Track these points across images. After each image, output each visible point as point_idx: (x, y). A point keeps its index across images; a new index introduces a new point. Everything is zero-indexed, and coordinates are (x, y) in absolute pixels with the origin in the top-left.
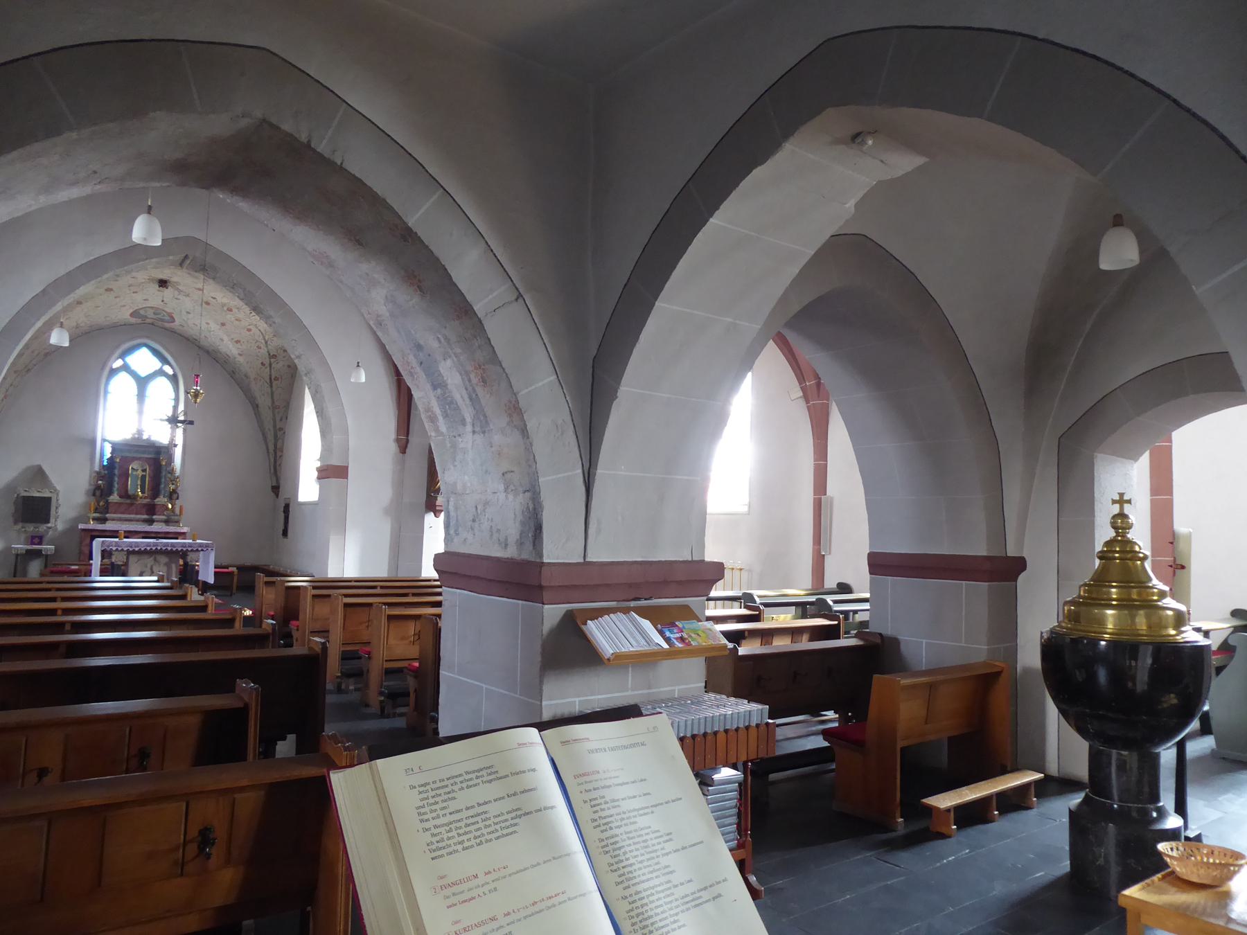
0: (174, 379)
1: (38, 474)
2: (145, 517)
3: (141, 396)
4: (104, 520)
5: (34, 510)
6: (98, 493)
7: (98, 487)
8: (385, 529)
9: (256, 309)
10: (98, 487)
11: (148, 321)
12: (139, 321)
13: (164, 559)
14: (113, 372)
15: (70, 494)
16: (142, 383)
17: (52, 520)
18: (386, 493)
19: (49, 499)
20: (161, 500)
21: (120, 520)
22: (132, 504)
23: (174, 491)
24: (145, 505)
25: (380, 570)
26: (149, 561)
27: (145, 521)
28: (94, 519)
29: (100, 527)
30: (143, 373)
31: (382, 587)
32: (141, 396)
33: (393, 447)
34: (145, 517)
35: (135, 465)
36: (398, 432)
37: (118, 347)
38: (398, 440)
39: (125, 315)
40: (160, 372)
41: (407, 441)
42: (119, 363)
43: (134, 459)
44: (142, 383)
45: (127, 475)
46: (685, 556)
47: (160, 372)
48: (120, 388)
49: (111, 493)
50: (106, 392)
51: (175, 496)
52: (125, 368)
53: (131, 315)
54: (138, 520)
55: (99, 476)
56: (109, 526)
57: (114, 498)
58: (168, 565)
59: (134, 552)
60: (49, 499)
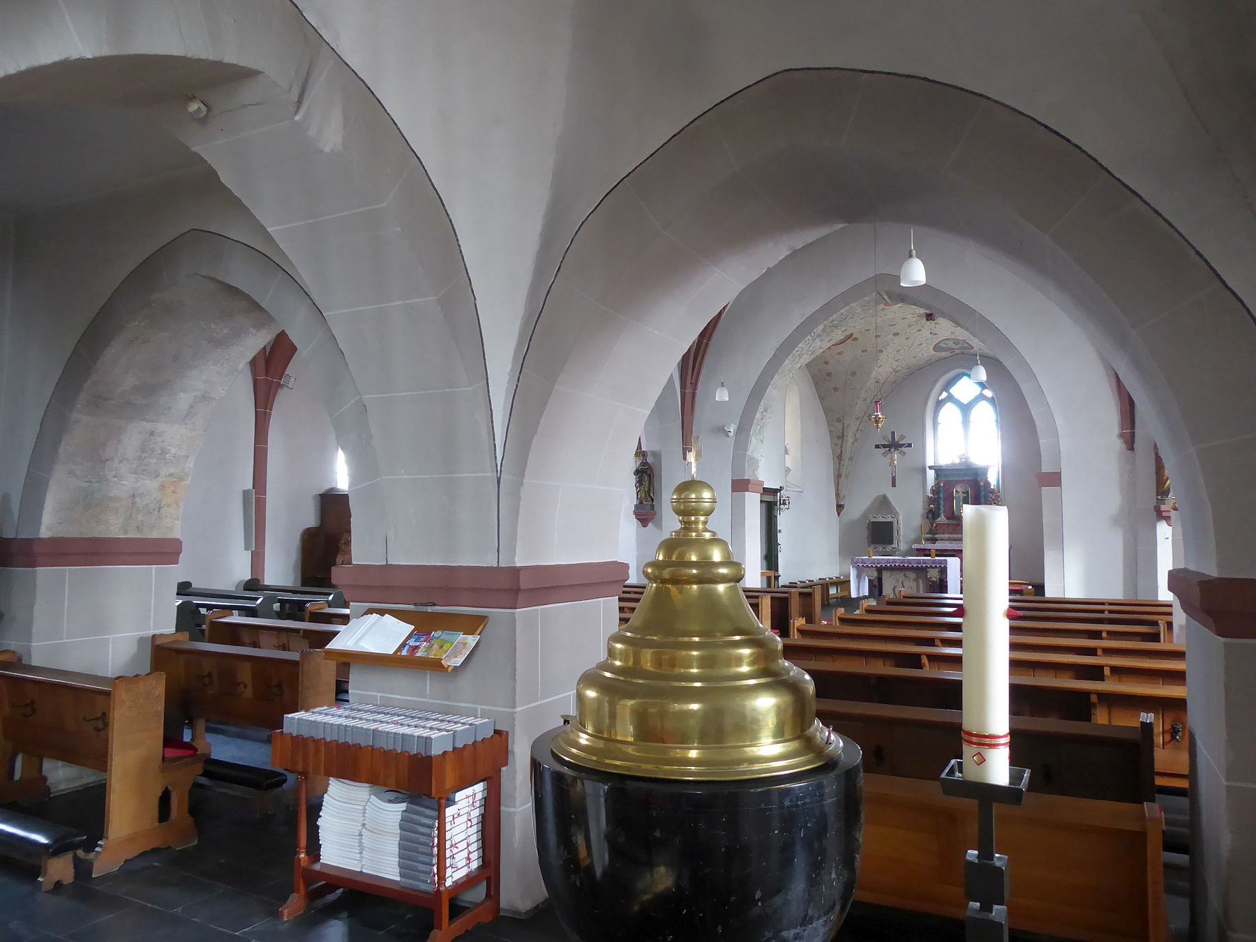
0: (992, 401)
1: (883, 503)
3: (966, 421)
4: (934, 540)
5: (881, 534)
7: (931, 511)
8: (1116, 542)
9: (958, 324)
10: (931, 511)
11: (957, 351)
12: (949, 354)
13: (912, 575)
14: (939, 404)
15: (909, 518)
16: (966, 409)
17: (895, 541)
18: (1113, 499)
19: (891, 523)
21: (948, 539)
25: (1112, 589)
26: (900, 576)
28: (927, 540)
29: (929, 546)
30: (965, 401)
31: (1110, 612)
32: (966, 421)
33: (1118, 444)
35: (959, 488)
36: (1122, 427)
37: (936, 381)
38: (1121, 435)
39: (928, 352)
40: (981, 397)
41: (1133, 435)
42: (944, 395)
44: (966, 409)
46: (490, 561)
47: (981, 397)
48: (949, 414)
50: (935, 424)
52: (950, 398)
53: (935, 349)
55: (931, 501)
56: (939, 545)
57: (942, 519)
58: (916, 580)
59: (886, 568)
60: (891, 523)
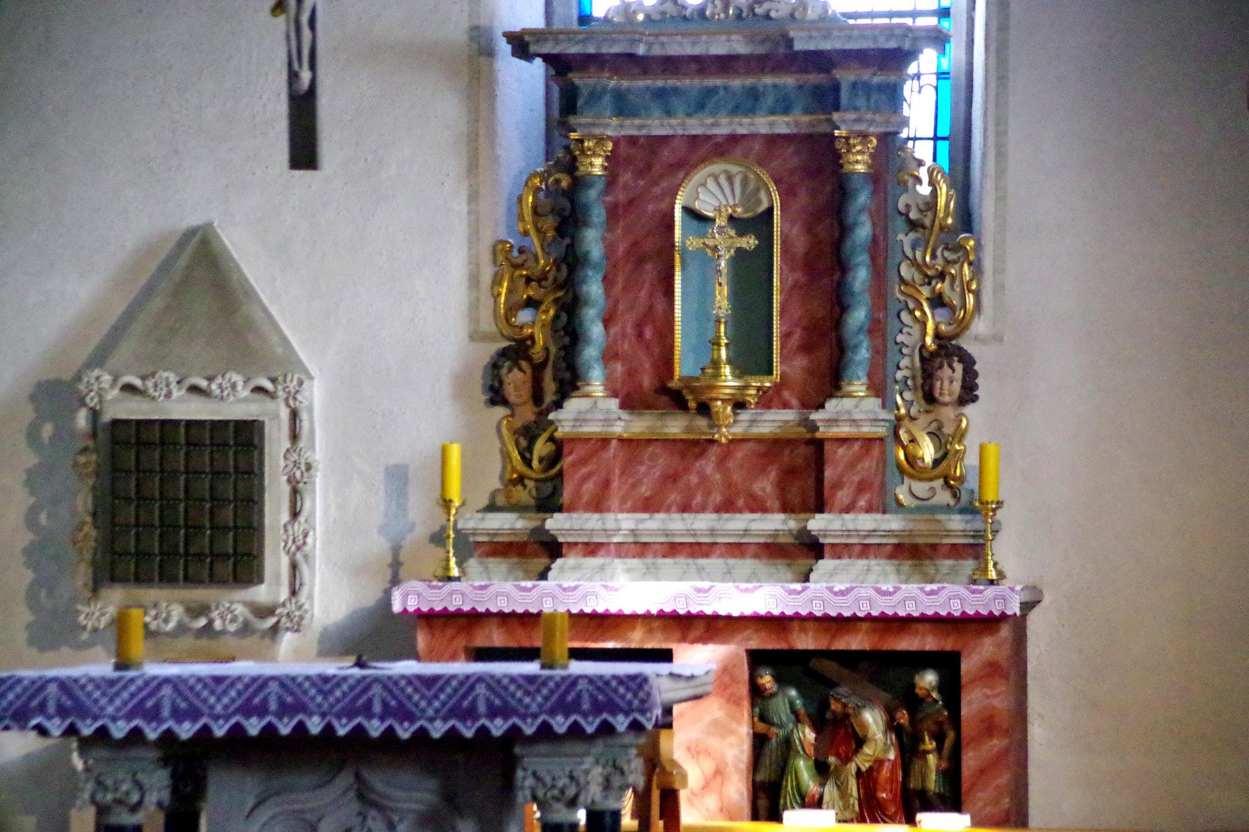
1: (196, 284)
2: (775, 523)
6: (516, 381)
10: (517, 351)
17: (275, 561)
19: (245, 438)
20: (854, 411)
21: (641, 549)
22: (694, 447)
23: (947, 349)
24: (773, 447)
27: (773, 550)
34: (775, 523)
35: (709, 192)
43: (703, 150)
45: (653, 257)
49: (571, 383)
51: (949, 381)
54: (737, 549)
57: (593, 410)
60: (245, 438)
